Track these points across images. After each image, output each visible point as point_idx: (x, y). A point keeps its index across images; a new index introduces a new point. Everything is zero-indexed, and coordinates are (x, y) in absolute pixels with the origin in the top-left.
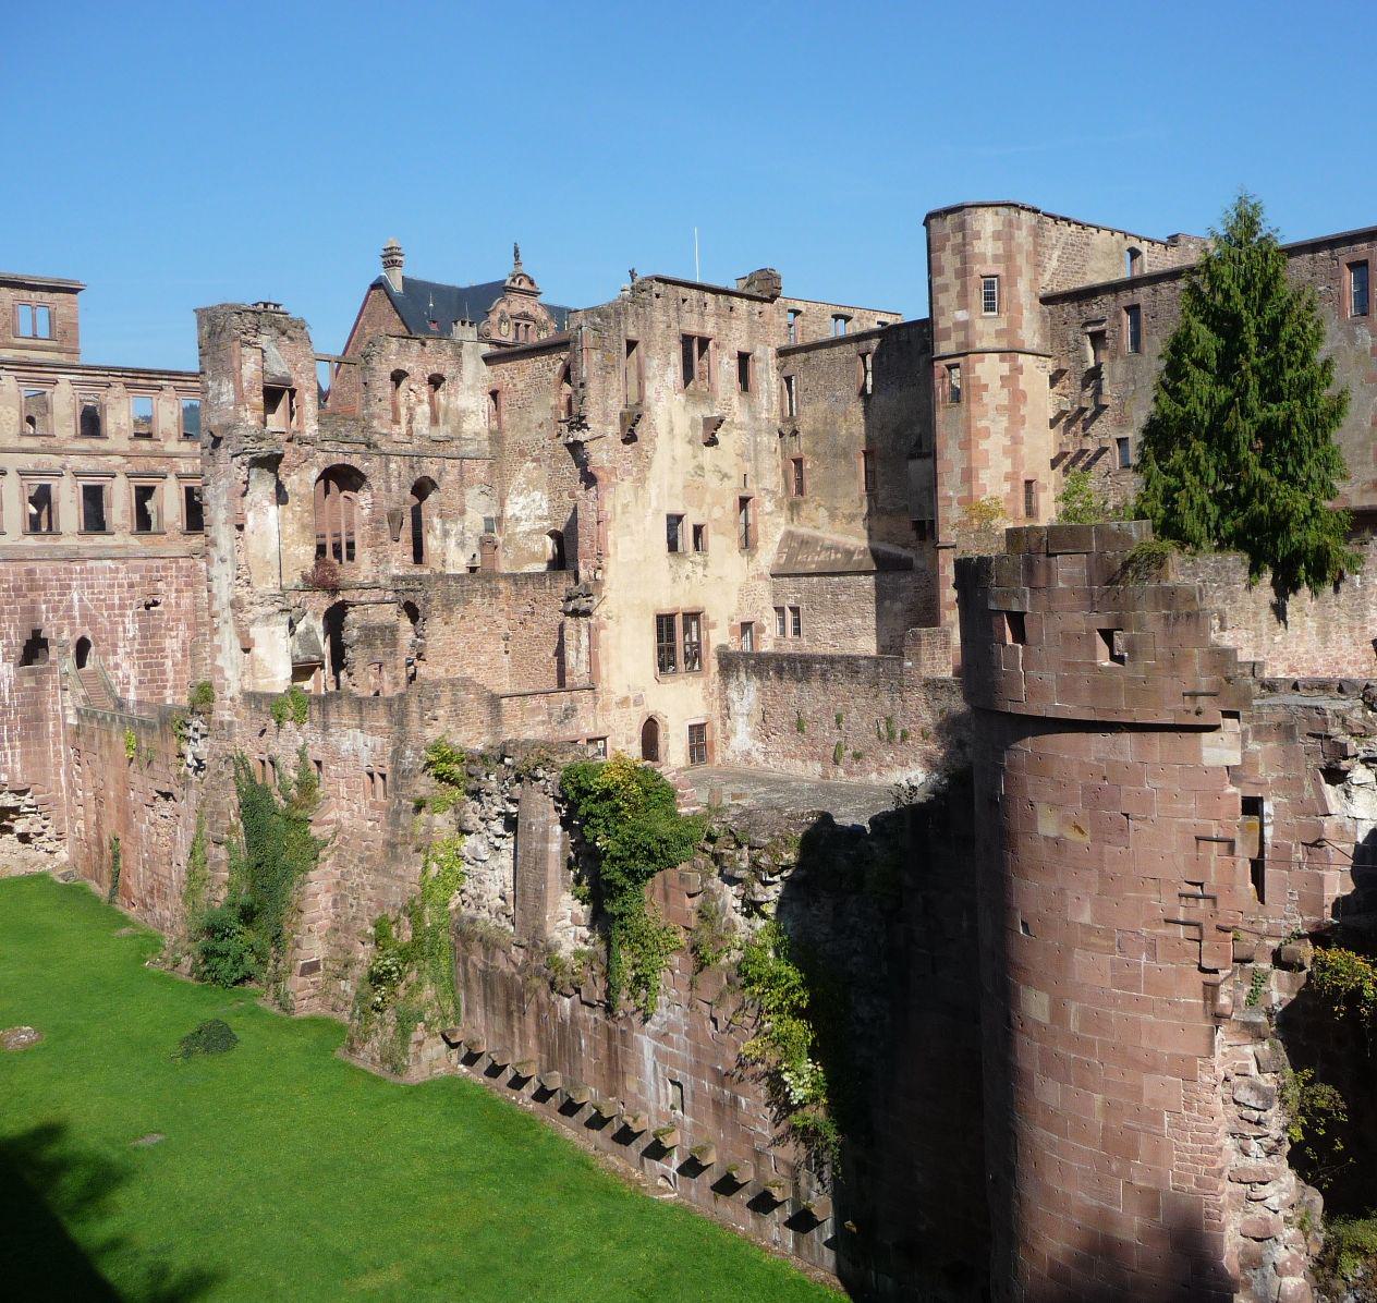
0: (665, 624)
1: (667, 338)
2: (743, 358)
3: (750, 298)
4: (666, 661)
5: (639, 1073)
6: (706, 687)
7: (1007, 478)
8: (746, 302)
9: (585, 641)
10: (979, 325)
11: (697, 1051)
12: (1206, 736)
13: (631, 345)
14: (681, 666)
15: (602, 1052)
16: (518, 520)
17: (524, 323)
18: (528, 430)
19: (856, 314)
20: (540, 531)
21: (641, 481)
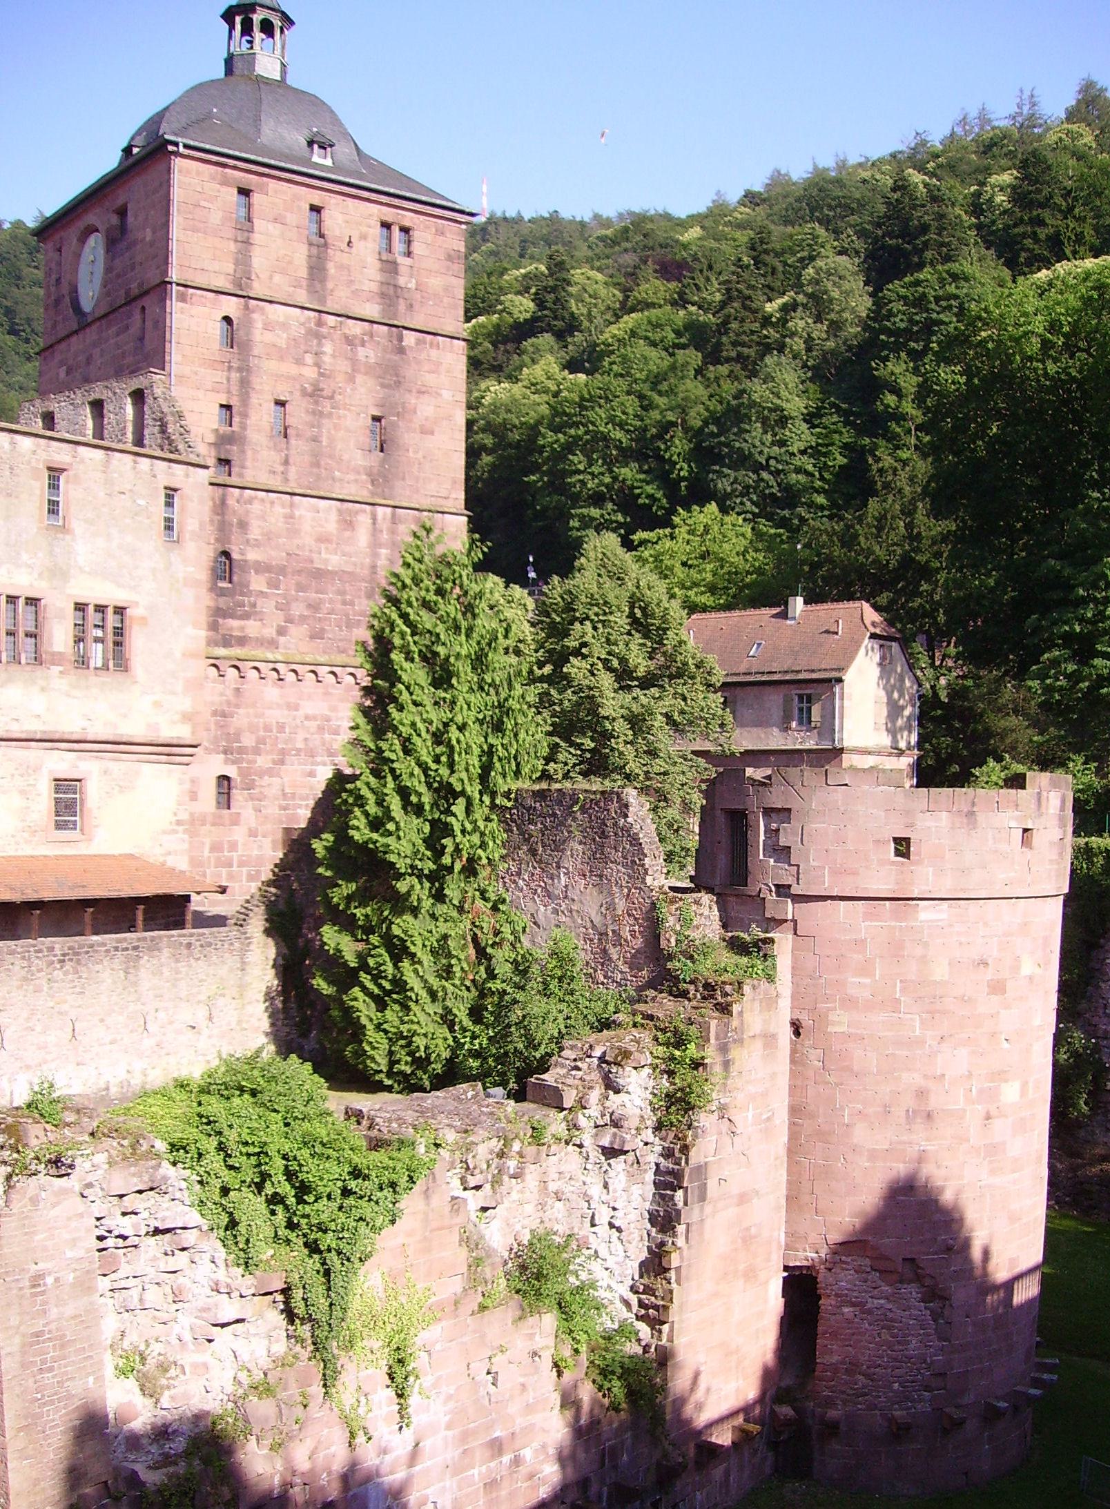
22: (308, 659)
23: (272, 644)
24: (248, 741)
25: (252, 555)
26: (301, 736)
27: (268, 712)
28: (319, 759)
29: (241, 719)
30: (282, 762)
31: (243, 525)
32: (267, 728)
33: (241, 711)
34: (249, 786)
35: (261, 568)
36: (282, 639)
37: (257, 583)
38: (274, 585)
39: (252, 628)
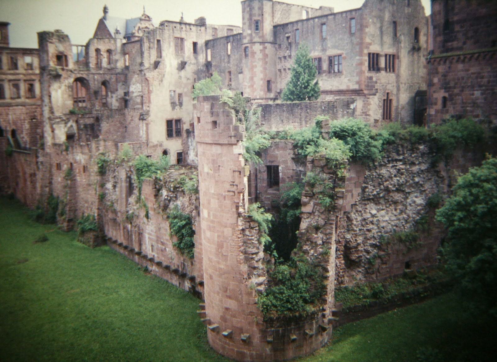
0: (169, 123)
1: (169, 37)
2: (195, 44)
3: (197, 25)
4: (170, 134)
5: (145, 244)
6: (183, 141)
7: (262, 79)
8: (195, 27)
9: (145, 128)
10: (254, 35)
11: (157, 237)
12: (234, 146)
13: (159, 41)
14: (174, 135)
15: (137, 239)
16: (133, 92)
17: (146, 30)
18: (136, 65)
19: (234, 28)
20: (139, 96)
21: (162, 81)
22: (471, 52)
23: (460, 49)
24: (452, 84)
25: (456, 18)
26: (470, 80)
27: (459, 73)
28: (476, 89)
29: (451, 76)
30: (462, 91)
31: (453, 9)
32: (458, 79)
33: (450, 74)
34: (452, 100)
35: (458, 22)
36: (465, 46)
37: (457, 28)
38: (462, 27)
39: (455, 44)
